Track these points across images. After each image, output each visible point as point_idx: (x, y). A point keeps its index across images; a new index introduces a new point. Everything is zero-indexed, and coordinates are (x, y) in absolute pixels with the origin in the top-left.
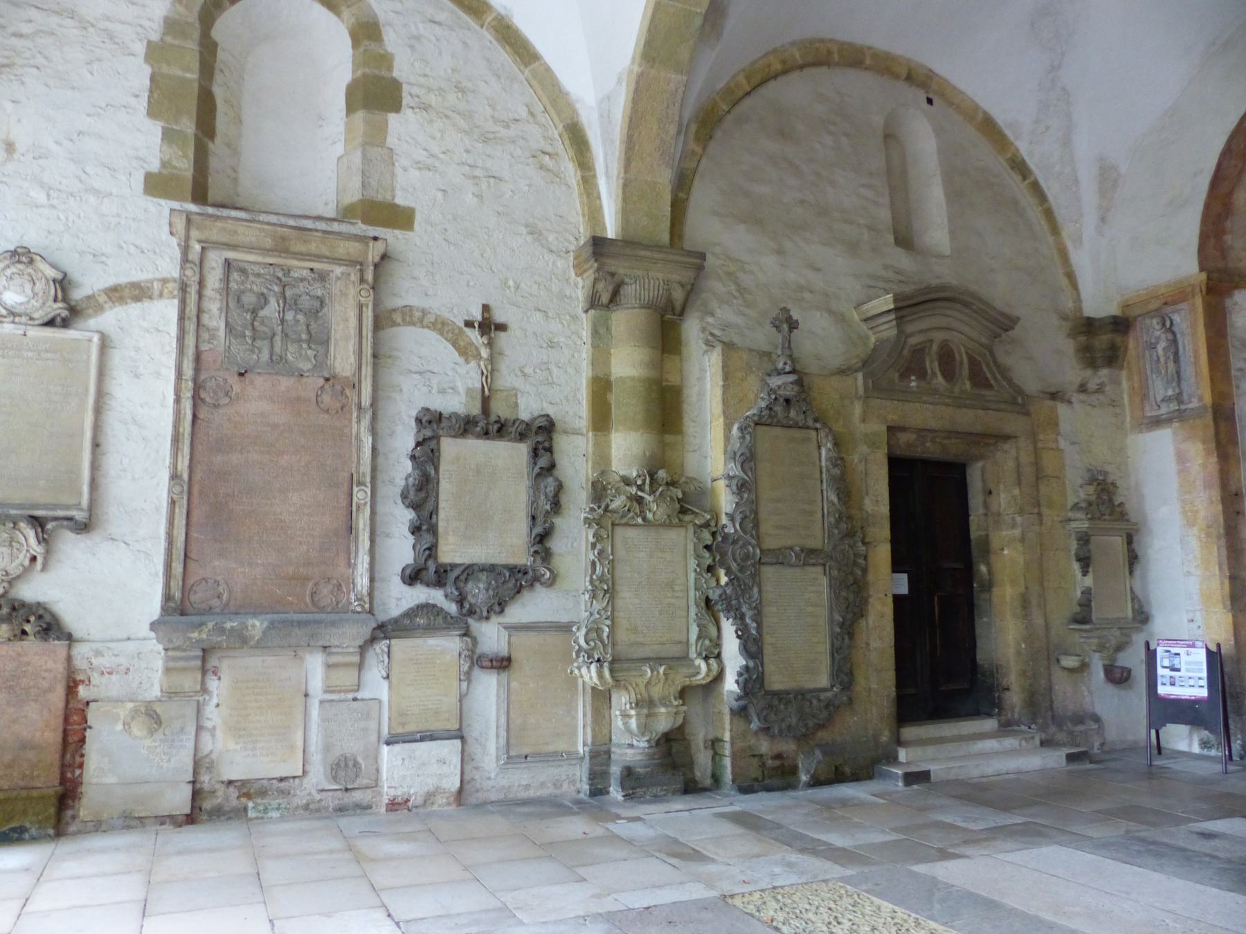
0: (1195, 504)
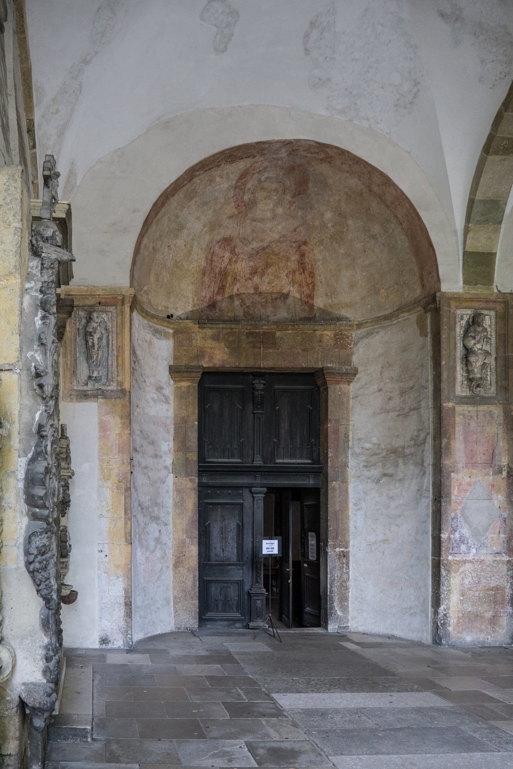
0: (111, 463)
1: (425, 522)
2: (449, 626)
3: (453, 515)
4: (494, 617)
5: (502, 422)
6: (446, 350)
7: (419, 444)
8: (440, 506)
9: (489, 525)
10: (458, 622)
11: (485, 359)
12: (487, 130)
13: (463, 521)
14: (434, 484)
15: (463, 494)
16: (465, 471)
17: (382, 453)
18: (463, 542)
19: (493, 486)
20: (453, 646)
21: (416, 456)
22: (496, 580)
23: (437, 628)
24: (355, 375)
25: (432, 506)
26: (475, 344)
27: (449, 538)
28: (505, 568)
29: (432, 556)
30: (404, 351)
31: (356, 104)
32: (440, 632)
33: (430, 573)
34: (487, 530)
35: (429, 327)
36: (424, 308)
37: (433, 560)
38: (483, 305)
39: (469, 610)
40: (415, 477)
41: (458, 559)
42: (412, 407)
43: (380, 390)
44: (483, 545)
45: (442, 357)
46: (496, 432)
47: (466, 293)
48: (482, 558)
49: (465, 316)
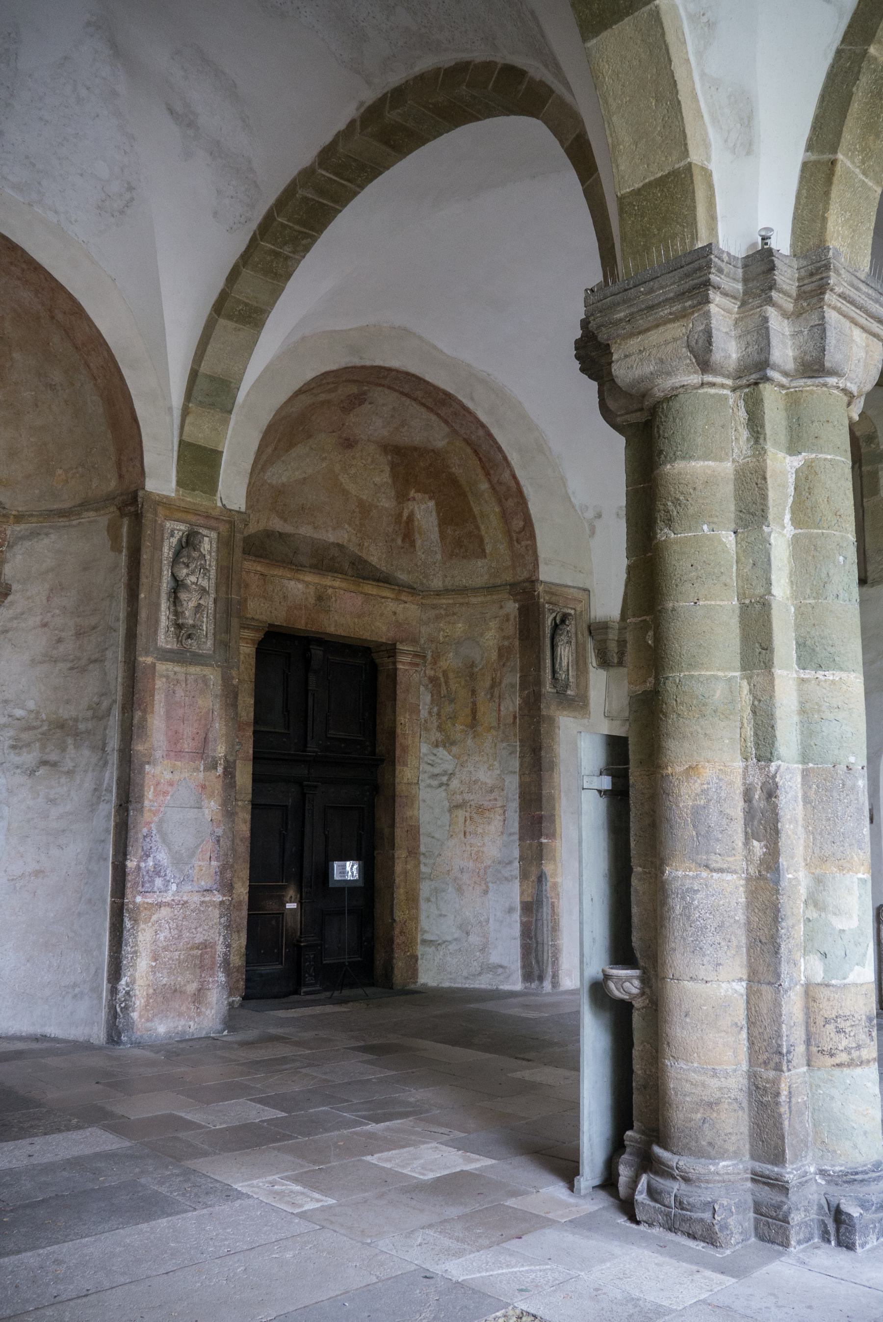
1: (103, 841)
2: (133, 1011)
3: (145, 831)
4: (199, 990)
5: (219, 693)
6: (147, 577)
7: (99, 716)
8: (127, 815)
9: (197, 847)
10: (147, 1004)
11: (200, 598)
12: (220, 283)
13: (160, 841)
14: (119, 780)
15: (161, 798)
16: (165, 762)
17: (41, 726)
18: (158, 874)
19: (204, 787)
20: (138, 1044)
21: (94, 734)
22: (204, 932)
23: (115, 1016)
24: (6, 595)
25: (115, 816)
26: (188, 575)
27: (139, 868)
28: (217, 912)
29: (112, 897)
30: (85, 569)
31: (39, 183)
32: (120, 1022)
33: (107, 924)
34: (192, 855)
35: (125, 539)
36: (119, 509)
37: (113, 903)
38: (201, 521)
39: (165, 982)
40: (91, 769)
41: (150, 901)
42: (93, 657)
43: (45, 625)
44: (186, 879)
45: (141, 587)
46: (211, 707)
47: (179, 499)
48: (185, 898)
49: (176, 532)
